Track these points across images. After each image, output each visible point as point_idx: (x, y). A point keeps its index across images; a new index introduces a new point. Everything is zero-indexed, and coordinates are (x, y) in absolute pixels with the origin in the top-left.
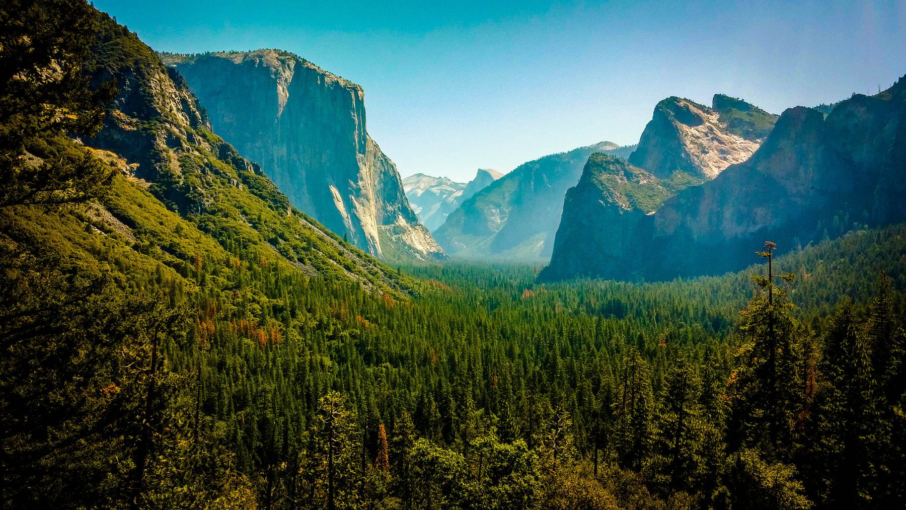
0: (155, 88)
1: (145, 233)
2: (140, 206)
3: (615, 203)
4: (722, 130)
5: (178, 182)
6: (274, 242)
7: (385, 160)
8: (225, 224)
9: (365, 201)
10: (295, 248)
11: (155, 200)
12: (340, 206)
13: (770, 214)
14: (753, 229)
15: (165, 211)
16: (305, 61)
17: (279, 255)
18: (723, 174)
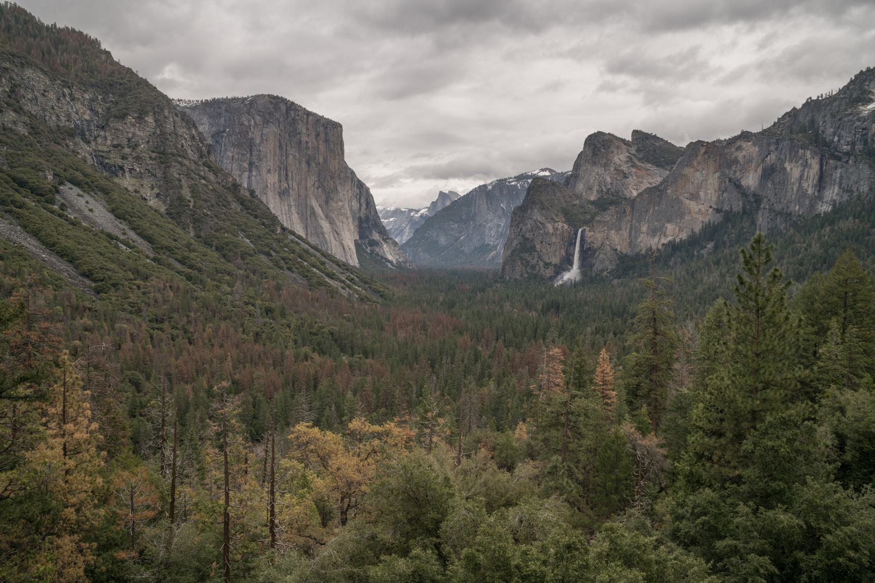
0: (169, 127)
1: (162, 248)
2: (157, 225)
3: (553, 219)
4: (640, 160)
5: (189, 206)
6: (268, 254)
7: (361, 185)
8: (226, 240)
9: (345, 220)
10: (284, 259)
11: (170, 220)
12: (325, 225)
13: (677, 229)
14: (664, 241)
15: (179, 230)
16: (293, 103)
17: (271, 264)
18: (640, 195)
